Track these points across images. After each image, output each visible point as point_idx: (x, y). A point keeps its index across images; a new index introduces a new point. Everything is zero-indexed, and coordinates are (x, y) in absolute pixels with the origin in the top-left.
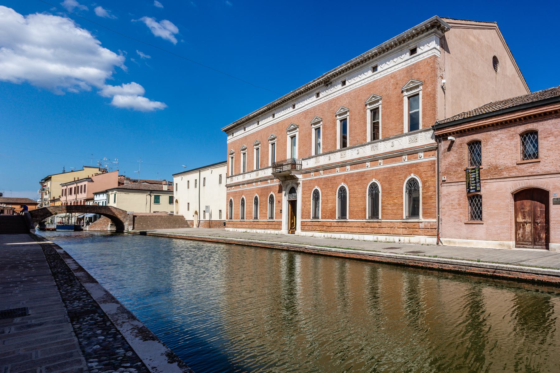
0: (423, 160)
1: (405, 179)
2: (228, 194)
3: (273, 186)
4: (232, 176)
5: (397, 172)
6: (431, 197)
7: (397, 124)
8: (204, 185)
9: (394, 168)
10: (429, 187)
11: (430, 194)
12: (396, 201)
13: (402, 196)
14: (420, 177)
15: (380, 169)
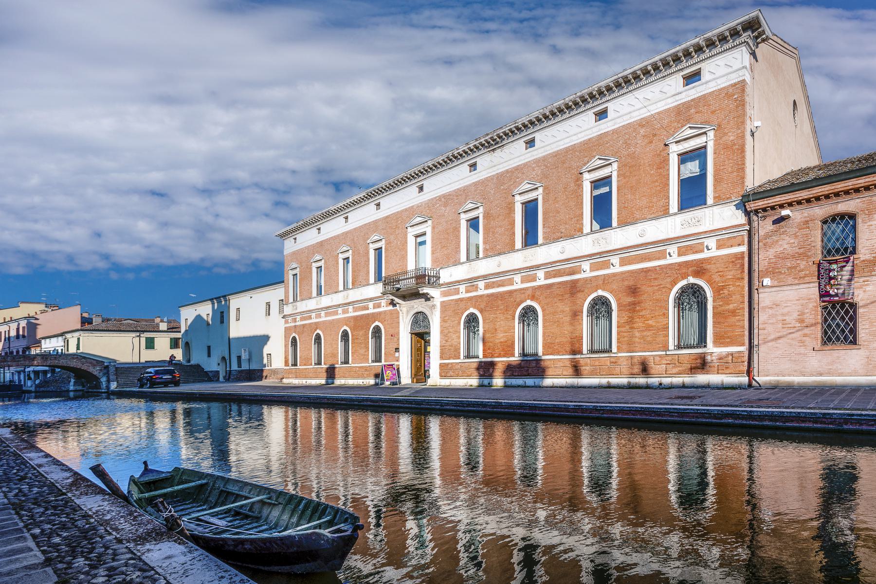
0: (714, 253)
1: (673, 286)
2: (287, 330)
3: (380, 313)
4: (295, 300)
5: (654, 276)
6: (733, 313)
7: (655, 200)
8: (238, 319)
9: (646, 271)
10: (730, 295)
11: (731, 307)
12: (650, 322)
13: (666, 315)
14: (709, 282)
15: (614, 275)
